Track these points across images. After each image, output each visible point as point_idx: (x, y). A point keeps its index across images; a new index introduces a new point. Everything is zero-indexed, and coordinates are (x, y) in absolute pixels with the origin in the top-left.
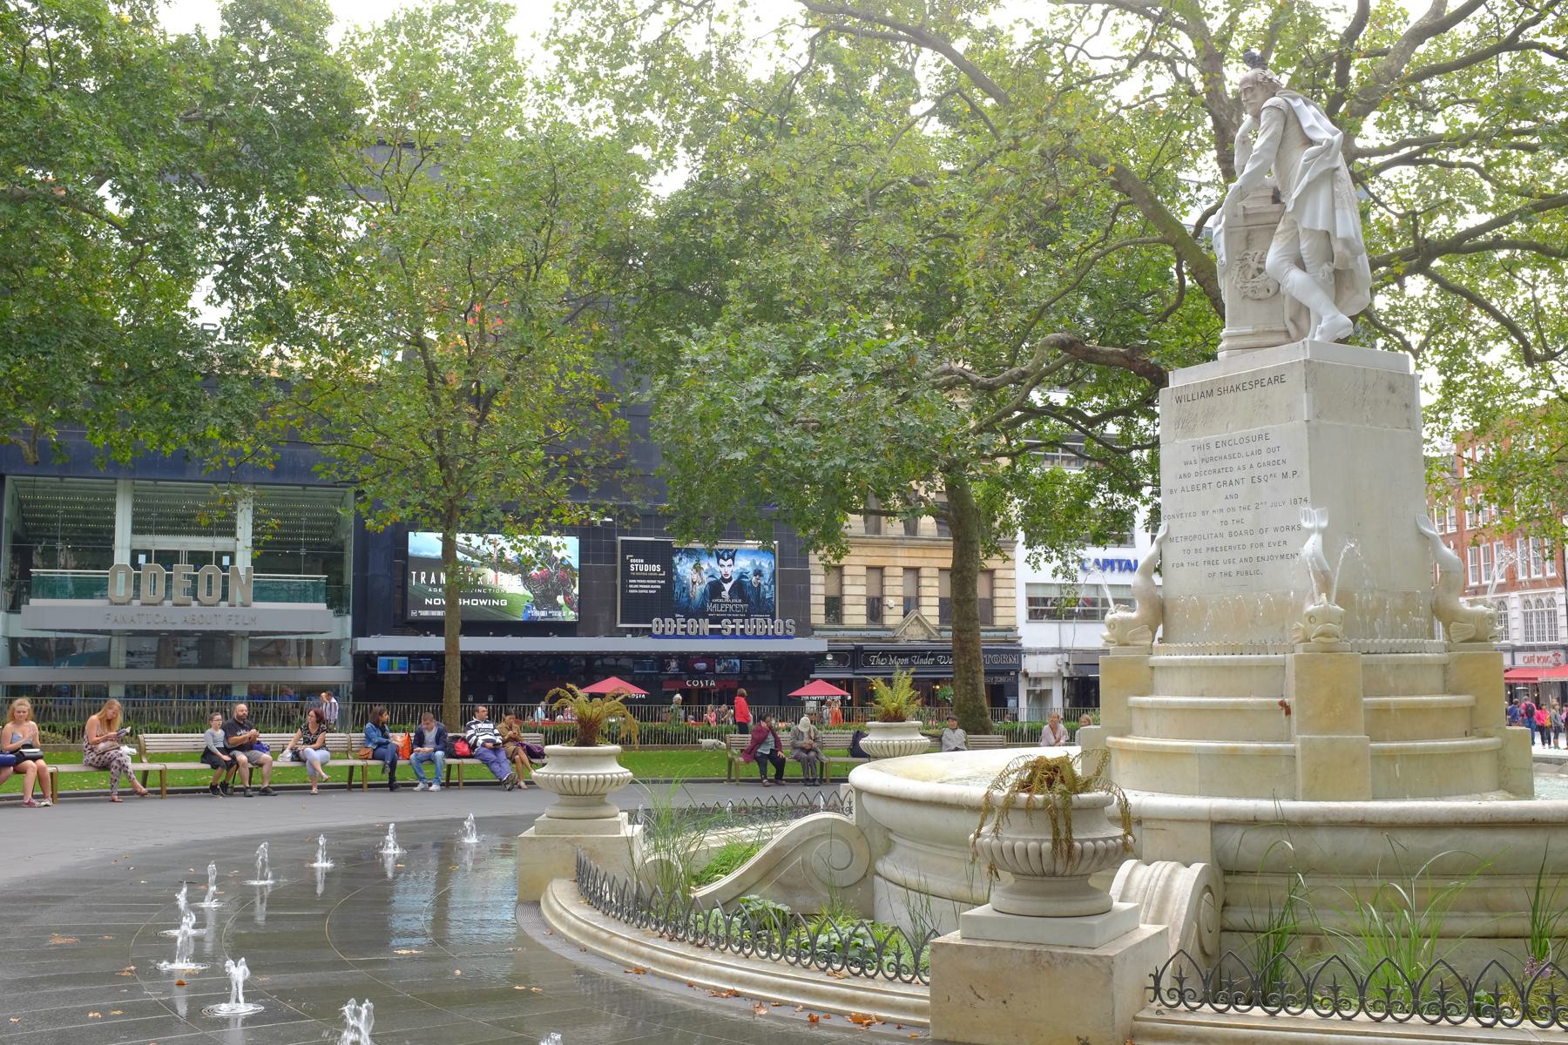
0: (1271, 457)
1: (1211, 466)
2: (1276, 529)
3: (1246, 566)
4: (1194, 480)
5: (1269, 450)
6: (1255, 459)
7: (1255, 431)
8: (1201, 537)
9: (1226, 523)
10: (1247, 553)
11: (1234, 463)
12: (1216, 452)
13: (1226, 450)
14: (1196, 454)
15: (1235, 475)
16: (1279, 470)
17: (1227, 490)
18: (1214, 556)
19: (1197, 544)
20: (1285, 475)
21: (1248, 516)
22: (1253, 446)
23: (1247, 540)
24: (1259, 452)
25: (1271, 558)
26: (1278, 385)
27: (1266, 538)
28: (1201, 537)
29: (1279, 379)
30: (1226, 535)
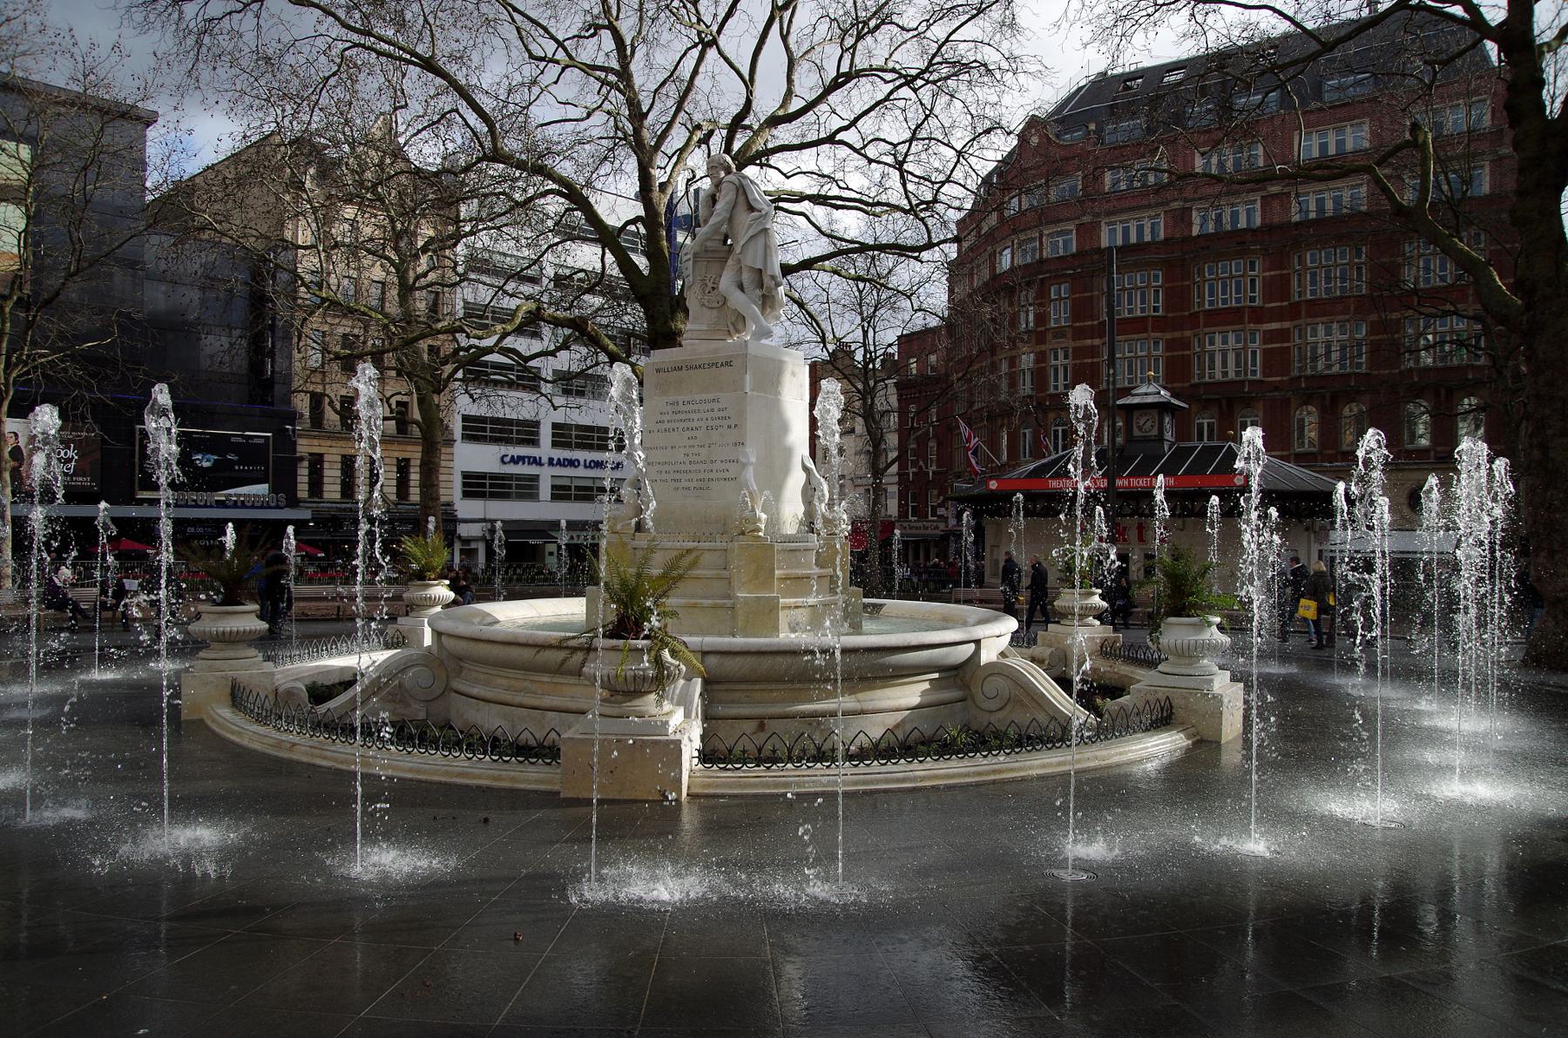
0: (721, 414)
4: (667, 425)
7: (711, 396)
8: (669, 463)
13: (690, 407)
14: (669, 409)
16: (725, 423)
18: (678, 476)
19: (666, 468)
21: (703, 451)
22: (709, 406)
23: (702, 467)
27: (714, 467)
28: (669, 463)
29: (729, 364)
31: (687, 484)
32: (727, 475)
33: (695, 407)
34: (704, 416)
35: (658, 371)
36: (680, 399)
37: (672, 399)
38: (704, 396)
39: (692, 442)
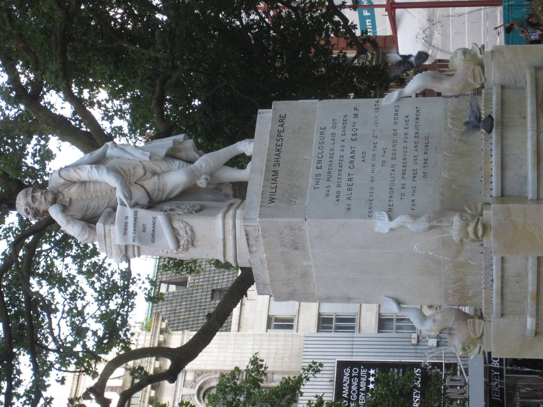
0: (340, 125)
1: (335, 173)
2: (396, 123)
3: (421, 148)
6: (338, 137)
7: (316, 137)
10: (411, 145)
12: (325, 169)
14: (323, 184)
15: (347, 154)
16: (351, 119)
18: (409, 173)
19: (397, 187)
20: (356, 116)
21: (382, 144)
24: (333, 135)
25: (417, 127)
26: (286, 120)
27: (401, 131)
28: (392, 184)
30: (394, 162)
31: (420, 162)
32: (412, 118)
33: (326, 152)
34: (338, 143)
35: (272, 200)
36: (313, 171)
37: (311, 181)
39: (369, 157)
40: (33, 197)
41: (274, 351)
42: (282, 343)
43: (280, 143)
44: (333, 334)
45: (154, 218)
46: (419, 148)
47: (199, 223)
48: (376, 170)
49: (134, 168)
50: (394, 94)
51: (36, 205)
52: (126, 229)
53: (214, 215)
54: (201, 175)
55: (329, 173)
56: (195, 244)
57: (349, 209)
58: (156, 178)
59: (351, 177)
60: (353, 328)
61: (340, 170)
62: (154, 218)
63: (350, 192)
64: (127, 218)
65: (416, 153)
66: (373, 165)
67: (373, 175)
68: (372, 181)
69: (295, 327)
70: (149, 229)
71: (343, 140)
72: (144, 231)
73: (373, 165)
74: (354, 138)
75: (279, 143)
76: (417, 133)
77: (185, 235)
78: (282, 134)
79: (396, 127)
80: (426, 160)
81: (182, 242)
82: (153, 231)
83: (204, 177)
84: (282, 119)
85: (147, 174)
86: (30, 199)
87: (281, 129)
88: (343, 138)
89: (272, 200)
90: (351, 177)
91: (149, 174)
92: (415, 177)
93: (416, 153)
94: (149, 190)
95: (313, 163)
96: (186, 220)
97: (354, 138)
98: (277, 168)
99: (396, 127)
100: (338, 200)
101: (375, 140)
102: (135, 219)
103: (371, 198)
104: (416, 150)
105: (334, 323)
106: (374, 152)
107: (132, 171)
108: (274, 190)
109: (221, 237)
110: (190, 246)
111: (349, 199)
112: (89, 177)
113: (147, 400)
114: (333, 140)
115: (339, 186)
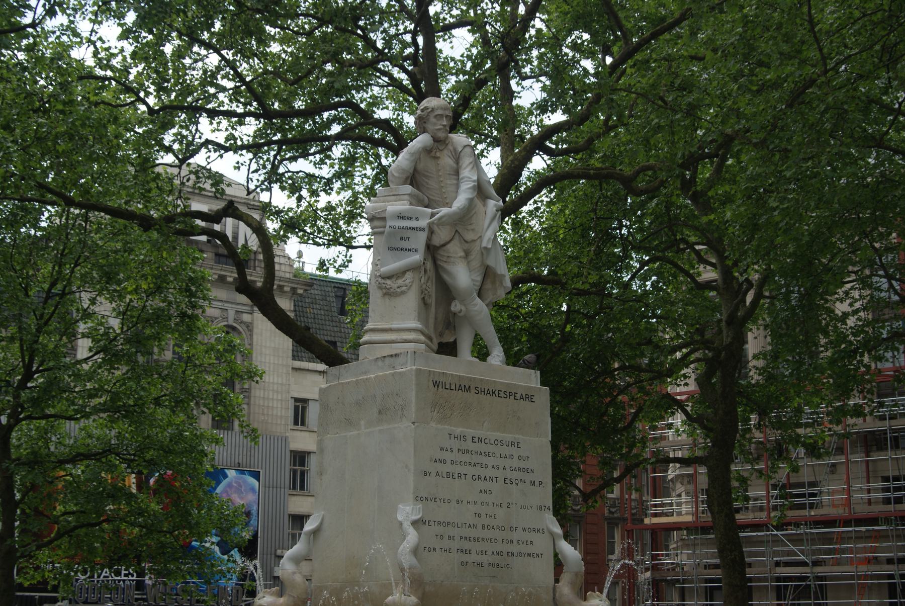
0: (522, 464)
2: (524, 530)
3: (497, 559)
5: (520, 458)
6: (508, 463)
7: (509, 437)
9: (480, 516)
10: (499, 547)
11: (490, 461)
13: (482, 447)
15: (489, 472)
16: (529, 477)
17: (481, 485)
18: (466, 545)
19: (451, 531)
20: (533, 483)
21: (500, 512)
23: (498, 534)
24: (511, 457)
25: (519, 554)
26: (527, 403)
27: (515, 536)
30: (479, 527)
33: (491, 449)
35: (436, 384)
36: (470, 432)
37: (458, 430)
38: (498, 435)
39: (485, 497)
40: (441, 116)
41: (271, 405)
42: (279, 414)
43: (502, 394)
44: (288, 467)
45: (416, 251)
46: (495, 556)
47: (410, 301)
48: (470, 506)
49: (473, 230)
50: (558, 530)
51: (432, 120)
52: (403, 218)
53: (419, 319)
54: (465, 305)
55: (468, 451)
56: (387, 297)
57: (425, 474)
58: (462, 254)
59: (463, 476)
60: (294, 488)
61: (470, 464)
62: (416, 251)
63: (444, 475)
64: (417, 219)
65: (489, 553)
66: (475, 503)
67: (465, 502)
68: (458, 502)
69: (296, 427)
70: (404, 244)
71: (504, 468)
72: (402, 239)
73: (475, 503)
74: (508, 481)
75: (502, 394)
76: (513, 554)
77: (396, 286)
78: (512, 397)
79: (520, 529)
80: (481, 565)
81: (389, 282)
82: (402, 249)
83: (463, 308)
84: (529, 398)
85: (467, 245)
86: (439, 112)
87: (518, 396)
88: (507, 468)
89: (436, 384)
90: (463, 476)
91: (466, 246)
92: (462, 551)
93: (489, 553)
94: (448, 246)
95: (479, 433)
96: (414, 286)
97: (508, 481)
98: (473, 391)
99: (520, 529)
100: (435, 461)
101: (505, 505)
102: (415, 229)
103: (438, 500)
104: (493, 554)
105: (299, 468)
106: (491, 505)
107: (469, 227)
108: (448, 386)
109: (395, 326)
110: (384, 291)
111: (437, 474)
112: (463, 178)
113: (223, 273)
114: (506, 457)
115: (452, 462)
